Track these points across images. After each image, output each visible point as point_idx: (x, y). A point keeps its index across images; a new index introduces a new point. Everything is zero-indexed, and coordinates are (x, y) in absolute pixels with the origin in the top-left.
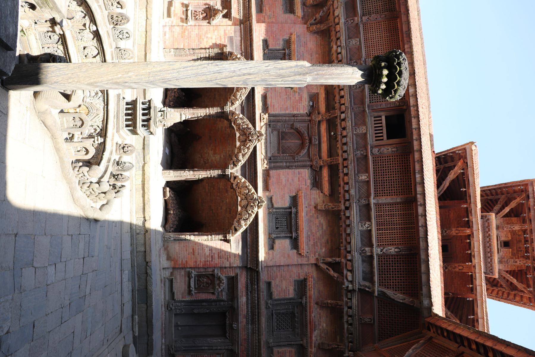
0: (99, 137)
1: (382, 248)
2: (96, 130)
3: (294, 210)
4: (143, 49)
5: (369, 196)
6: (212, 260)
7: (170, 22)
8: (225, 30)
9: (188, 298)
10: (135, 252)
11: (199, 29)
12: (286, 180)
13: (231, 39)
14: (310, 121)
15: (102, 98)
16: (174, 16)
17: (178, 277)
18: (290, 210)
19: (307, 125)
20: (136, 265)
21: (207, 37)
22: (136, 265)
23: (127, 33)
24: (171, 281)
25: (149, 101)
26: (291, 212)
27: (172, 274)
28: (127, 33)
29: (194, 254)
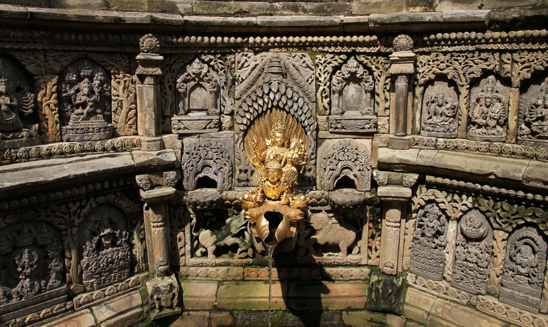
0: (395, 55)
2: (353, 78)
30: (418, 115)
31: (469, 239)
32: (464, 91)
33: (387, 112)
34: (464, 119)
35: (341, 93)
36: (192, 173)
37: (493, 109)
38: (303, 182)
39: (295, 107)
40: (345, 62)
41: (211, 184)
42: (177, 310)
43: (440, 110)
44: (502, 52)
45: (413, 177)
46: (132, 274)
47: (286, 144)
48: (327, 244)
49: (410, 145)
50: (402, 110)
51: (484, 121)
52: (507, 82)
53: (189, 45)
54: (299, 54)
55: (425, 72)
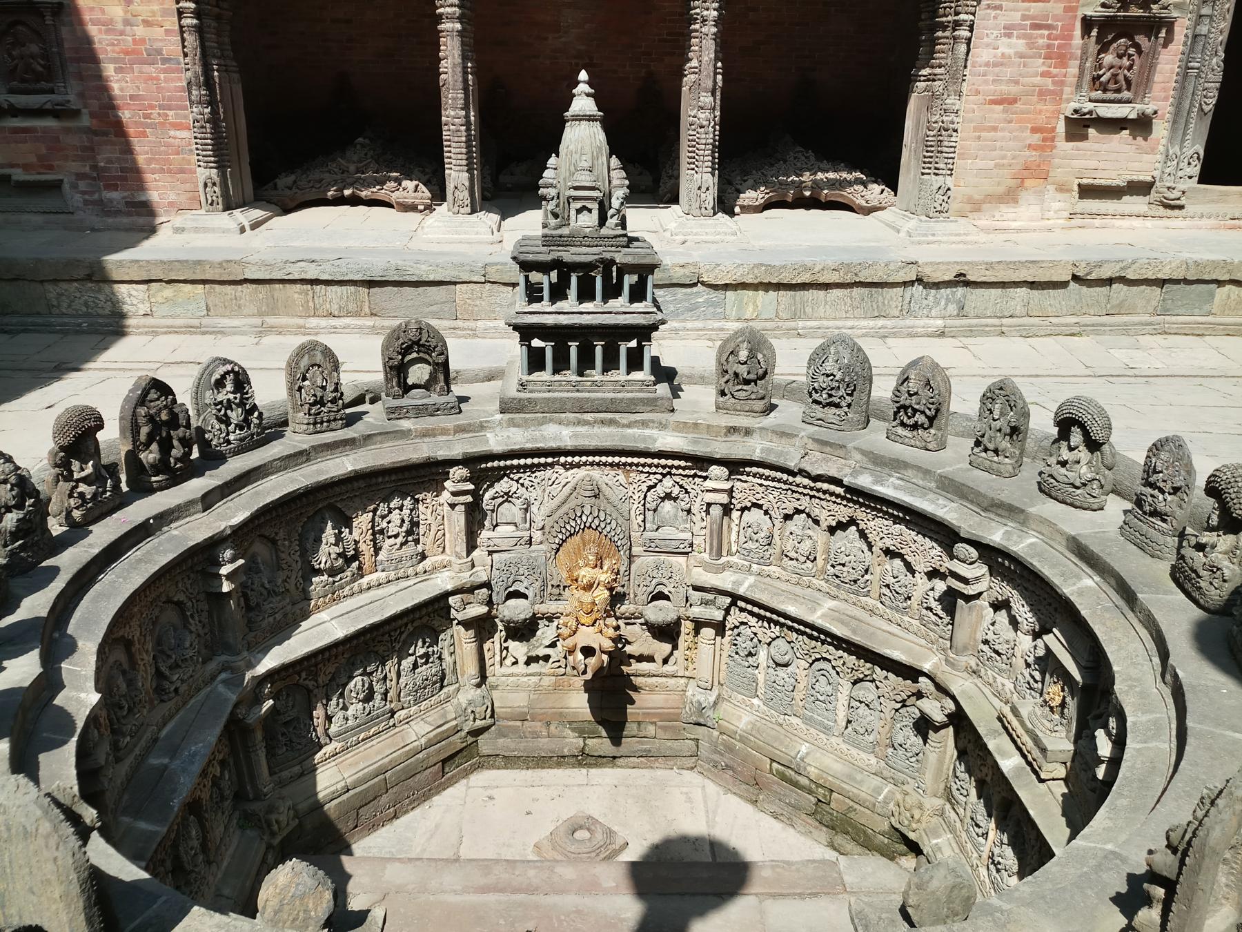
0: (709, 484)
2: (668, 496)
4: (229, 289)
6: (1048, 27)
7: (82, 185)
10: (1026, 320)
15: (525, 478)
16: (51, 167)
20: (1073, 320)
21: (127, 22)
22: (1073, 320)
23: (220, 384)
24: (1088, 191)
25: (526, 266)
27: (1062, 188)
28: (220, 384)
29: (1014, 101)
30: (734, 537)
31: (778, 665)
32: (778, 524)
33: (703, 532)
34: (778, 551)
35: (655, 510)
36: (503, 588)
37: (802, 546)
38: (617, 598)
39: (608, 528)
40: (661, 481)
41: (525, 596)
42: (489, 721)
43: (755, 537)
44: (811, 497)
45: (728, 600)
46: (442, 687)
47: (599, 563)
48: (641, 655)
49: (723, 568)
50: (715, 537)
51: (795, 555)
52: (817, 522)
53: (499, 468)
54: (613, 473)
55: (741, 499)
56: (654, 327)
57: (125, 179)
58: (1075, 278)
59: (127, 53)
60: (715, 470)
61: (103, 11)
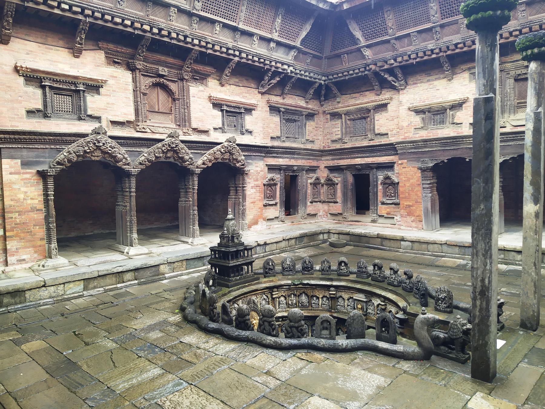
0: (274, 293)
1: (274, 31)
3: (225, 108)
5: (235, 29)
8: (11, 174)
9: (278, 205)
11: (12, 212)
12: (200, 112)
13: (25, 164)
14: (140, 71)
17: (266, 215)
18: (225, 112)
19: (142, 77)
21: (24, 199)
24: (268, 220)
26: (227, 111)
27: (264, 220)
56: (254, 261)
57: (18, 252)
58: (284, 240)
59: (24, 209)
60: (276, 290)
61: (16, 196)
